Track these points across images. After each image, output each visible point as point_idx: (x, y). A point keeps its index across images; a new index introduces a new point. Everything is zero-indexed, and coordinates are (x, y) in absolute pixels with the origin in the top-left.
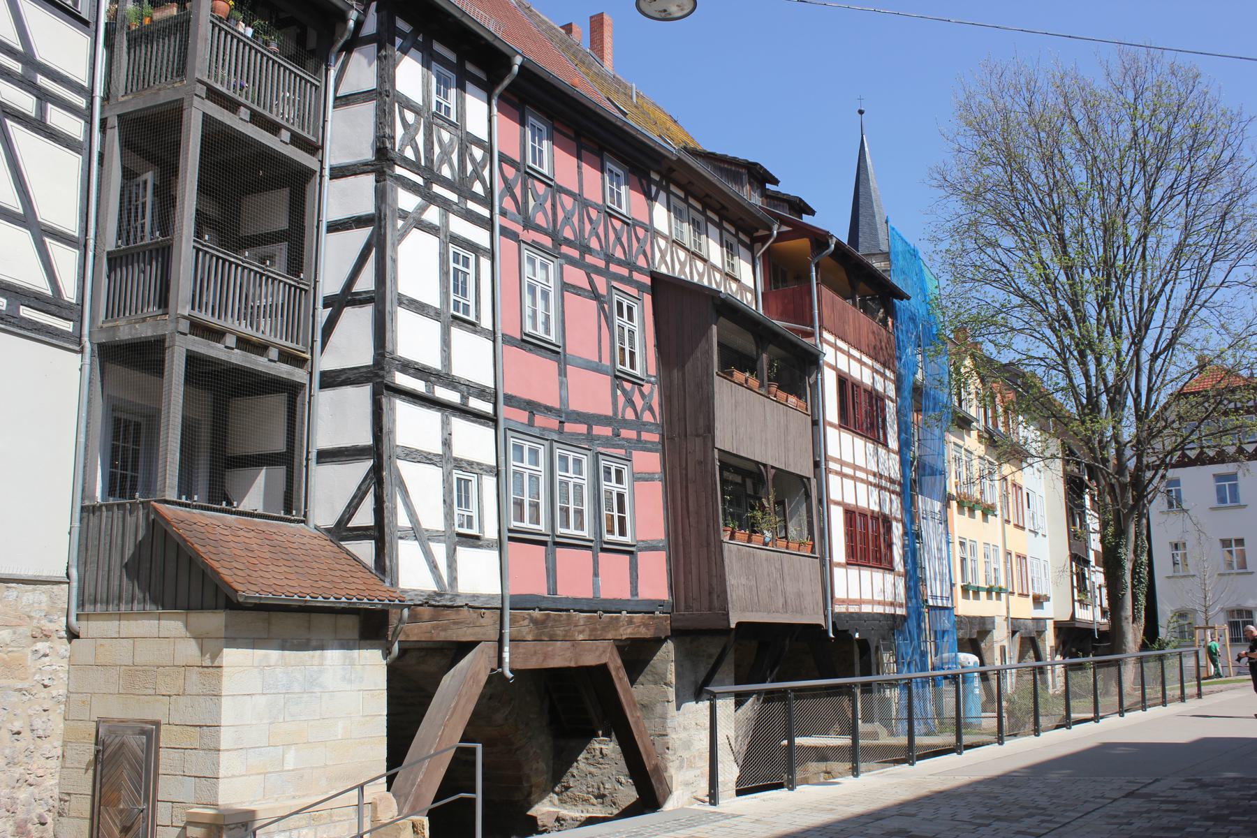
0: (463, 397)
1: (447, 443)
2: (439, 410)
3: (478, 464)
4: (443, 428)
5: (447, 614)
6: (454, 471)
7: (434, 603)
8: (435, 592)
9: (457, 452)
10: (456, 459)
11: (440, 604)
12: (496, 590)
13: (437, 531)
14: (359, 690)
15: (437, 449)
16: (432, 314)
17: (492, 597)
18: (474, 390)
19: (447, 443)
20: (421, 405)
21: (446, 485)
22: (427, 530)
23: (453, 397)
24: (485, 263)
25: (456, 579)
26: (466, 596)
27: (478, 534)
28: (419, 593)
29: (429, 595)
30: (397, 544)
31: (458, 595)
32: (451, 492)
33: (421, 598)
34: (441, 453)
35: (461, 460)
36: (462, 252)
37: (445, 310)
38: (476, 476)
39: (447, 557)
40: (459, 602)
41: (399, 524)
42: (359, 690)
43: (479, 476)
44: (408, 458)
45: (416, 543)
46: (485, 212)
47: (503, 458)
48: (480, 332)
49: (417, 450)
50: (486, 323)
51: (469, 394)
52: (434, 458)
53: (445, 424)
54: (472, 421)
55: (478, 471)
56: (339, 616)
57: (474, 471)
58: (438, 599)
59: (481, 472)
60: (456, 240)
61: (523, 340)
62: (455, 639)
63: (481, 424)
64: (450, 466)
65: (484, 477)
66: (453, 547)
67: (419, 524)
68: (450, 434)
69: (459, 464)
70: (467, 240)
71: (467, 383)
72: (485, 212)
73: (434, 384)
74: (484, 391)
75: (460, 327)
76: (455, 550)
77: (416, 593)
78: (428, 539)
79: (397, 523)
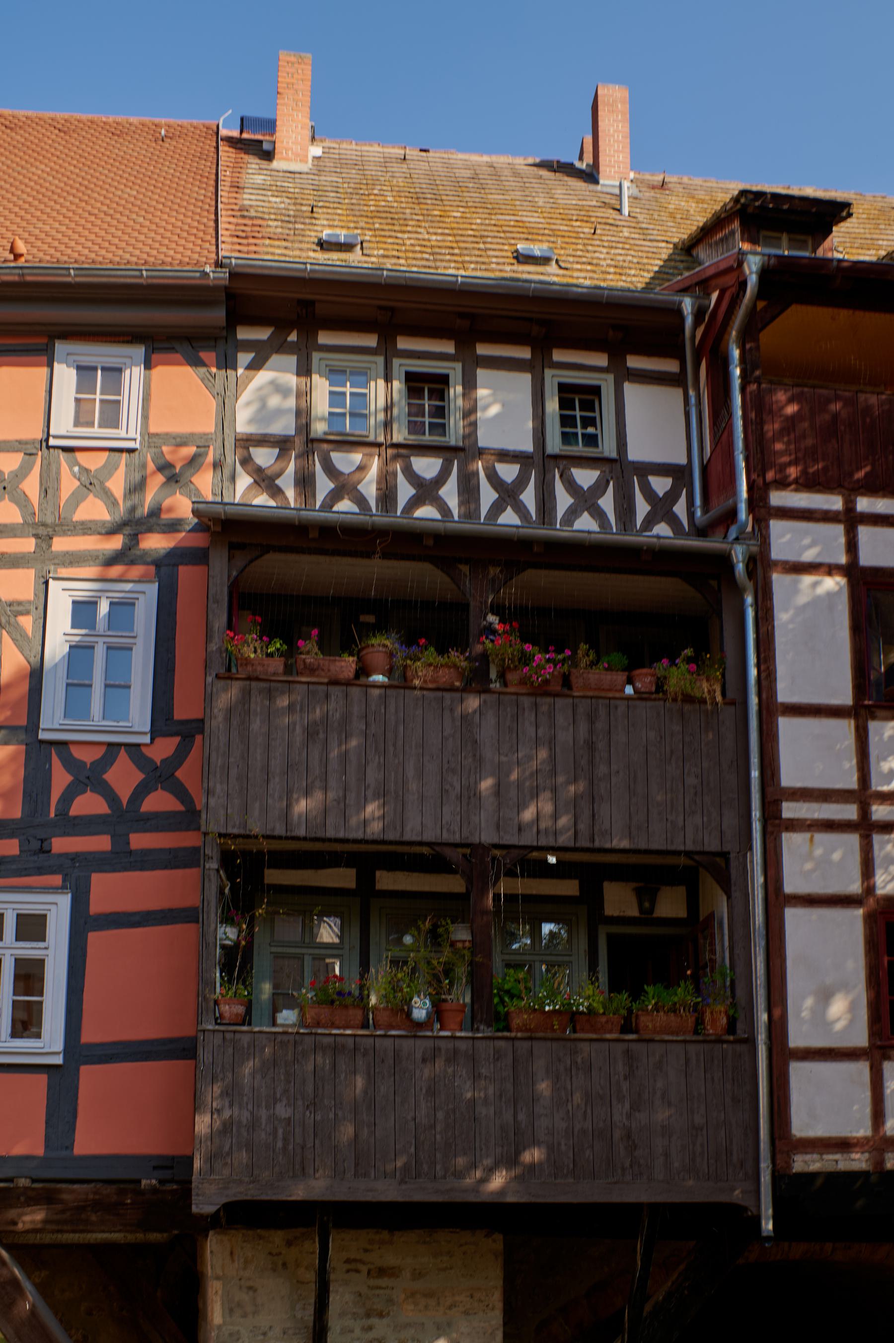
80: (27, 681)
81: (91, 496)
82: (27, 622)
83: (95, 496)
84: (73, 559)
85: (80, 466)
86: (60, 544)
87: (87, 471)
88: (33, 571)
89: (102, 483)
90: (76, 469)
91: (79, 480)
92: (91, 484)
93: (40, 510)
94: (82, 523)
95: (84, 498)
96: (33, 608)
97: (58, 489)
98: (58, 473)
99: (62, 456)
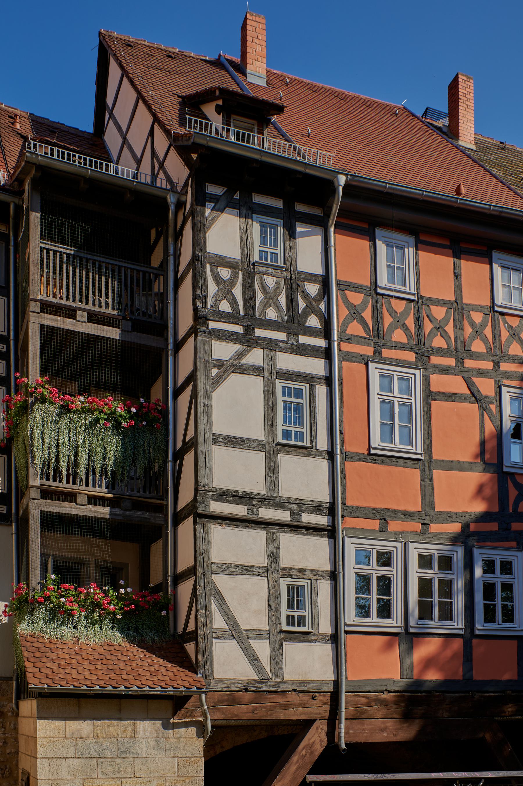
0: (293, 513)
1: (273, 556)
2: (264, 528)
3: (311, 571)
4: (268, 543)
5: (270, 698)
6: (282, 579)
7: (254, 689)
8: (255, 680)
9: (284, 562)
10: (283, 569)
11: (261, 690)
12: (330, 676)
13: (260, 630)
14: (174, 757)
15: (263, 561)
16: (255, 446)
17: (327, 683)
18: (308, 507)
19: (273, 556)
20: (243, 527)
21: (272, 592)
22: (247, 630)
23: (284, 516)
24: (321, 391)
25: (281, 669)
26: (293, 683)
27: (310, 630)
28: (236, 681)
29: (247, 683)
30: (212, 643)
31: (285, 683)
32: (278, 597)
33: (239, 686)
34: (266, 565)
35: (291, 569)
36: (293, 385)
37: (271, 441)
38: (309, 581)
39: (271, 651)
40: (283, 687)
41: (214, 627)
42: (174, 757)
43: (313, 582)
44: (225, 572)
45: (235, 641)
46: (321, 343)
47: (341, 563)
48: (316, 455)
49: (235, 565)
50: (323, 444)
51: (301, 511)
52: (258, 570)
53: (272, 539)
54: (307, 534)
55: (311, 577)
56: (150, 701)
57: (306, 577)
58: (258, 685)
59: (314, 577)
60: (283, 375)
61: (370, 454)
62: (282, 718)
63: (317, 535)
64: (276, 575)
65: (318, 581)
66: (278, 643)
67: (238, 625)
68: (278, 548)
69: (288, 573)
70: (299, 373)
71: (298, 502)
72: (321, 343)
73: (257, 507)
74: (320, 506)
75: (288, 452)
76: (281, 645)
77: (233, 681)
78: (248, 638)
79: (211, 627)
80: (496, 439)
81: (515, 342)
82: (493, 407)
83: (517, 342)
84: (509, 375)
85: (507, 323)
86: (504, 367)
87: (512, 327)
88: (493, 380)
89: (518, 335)
90: (506, 325)
91: (509, 332)
92: (514, 335)
93: (494, 347)
94: (513, 356)
95: (512, 343)
96: (494, 400)
97: (500, 336)
98: (499, 327)
99: (500, 317)
